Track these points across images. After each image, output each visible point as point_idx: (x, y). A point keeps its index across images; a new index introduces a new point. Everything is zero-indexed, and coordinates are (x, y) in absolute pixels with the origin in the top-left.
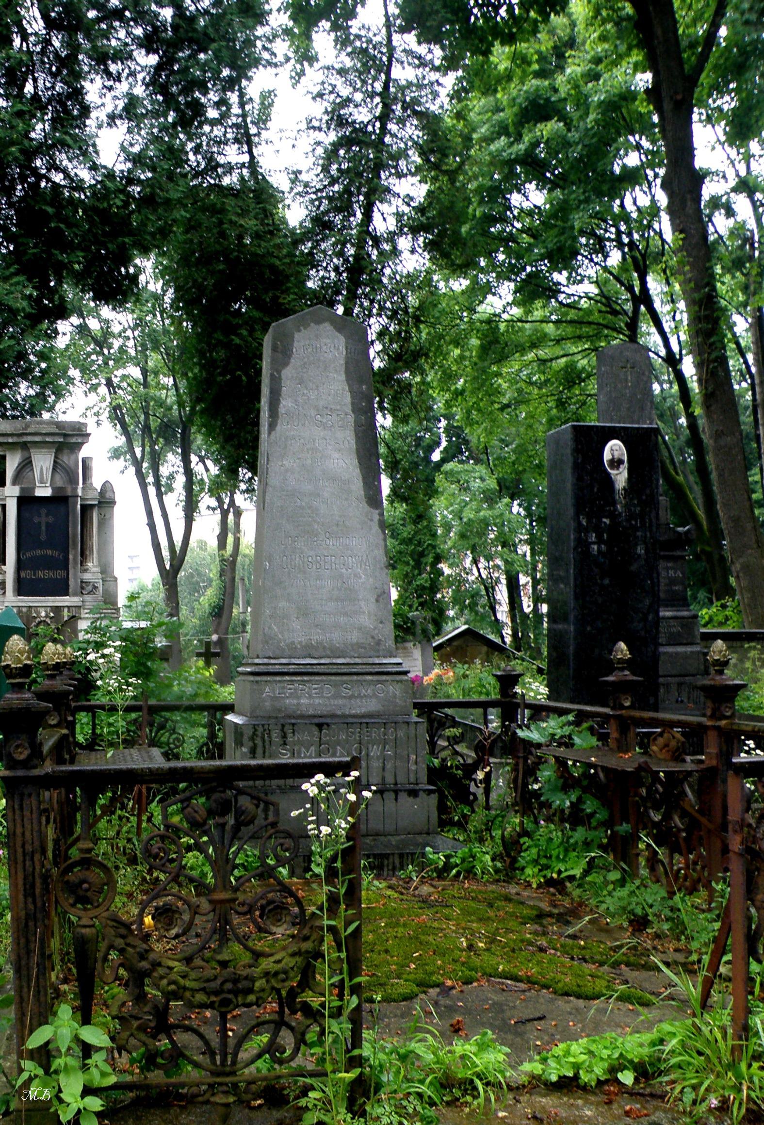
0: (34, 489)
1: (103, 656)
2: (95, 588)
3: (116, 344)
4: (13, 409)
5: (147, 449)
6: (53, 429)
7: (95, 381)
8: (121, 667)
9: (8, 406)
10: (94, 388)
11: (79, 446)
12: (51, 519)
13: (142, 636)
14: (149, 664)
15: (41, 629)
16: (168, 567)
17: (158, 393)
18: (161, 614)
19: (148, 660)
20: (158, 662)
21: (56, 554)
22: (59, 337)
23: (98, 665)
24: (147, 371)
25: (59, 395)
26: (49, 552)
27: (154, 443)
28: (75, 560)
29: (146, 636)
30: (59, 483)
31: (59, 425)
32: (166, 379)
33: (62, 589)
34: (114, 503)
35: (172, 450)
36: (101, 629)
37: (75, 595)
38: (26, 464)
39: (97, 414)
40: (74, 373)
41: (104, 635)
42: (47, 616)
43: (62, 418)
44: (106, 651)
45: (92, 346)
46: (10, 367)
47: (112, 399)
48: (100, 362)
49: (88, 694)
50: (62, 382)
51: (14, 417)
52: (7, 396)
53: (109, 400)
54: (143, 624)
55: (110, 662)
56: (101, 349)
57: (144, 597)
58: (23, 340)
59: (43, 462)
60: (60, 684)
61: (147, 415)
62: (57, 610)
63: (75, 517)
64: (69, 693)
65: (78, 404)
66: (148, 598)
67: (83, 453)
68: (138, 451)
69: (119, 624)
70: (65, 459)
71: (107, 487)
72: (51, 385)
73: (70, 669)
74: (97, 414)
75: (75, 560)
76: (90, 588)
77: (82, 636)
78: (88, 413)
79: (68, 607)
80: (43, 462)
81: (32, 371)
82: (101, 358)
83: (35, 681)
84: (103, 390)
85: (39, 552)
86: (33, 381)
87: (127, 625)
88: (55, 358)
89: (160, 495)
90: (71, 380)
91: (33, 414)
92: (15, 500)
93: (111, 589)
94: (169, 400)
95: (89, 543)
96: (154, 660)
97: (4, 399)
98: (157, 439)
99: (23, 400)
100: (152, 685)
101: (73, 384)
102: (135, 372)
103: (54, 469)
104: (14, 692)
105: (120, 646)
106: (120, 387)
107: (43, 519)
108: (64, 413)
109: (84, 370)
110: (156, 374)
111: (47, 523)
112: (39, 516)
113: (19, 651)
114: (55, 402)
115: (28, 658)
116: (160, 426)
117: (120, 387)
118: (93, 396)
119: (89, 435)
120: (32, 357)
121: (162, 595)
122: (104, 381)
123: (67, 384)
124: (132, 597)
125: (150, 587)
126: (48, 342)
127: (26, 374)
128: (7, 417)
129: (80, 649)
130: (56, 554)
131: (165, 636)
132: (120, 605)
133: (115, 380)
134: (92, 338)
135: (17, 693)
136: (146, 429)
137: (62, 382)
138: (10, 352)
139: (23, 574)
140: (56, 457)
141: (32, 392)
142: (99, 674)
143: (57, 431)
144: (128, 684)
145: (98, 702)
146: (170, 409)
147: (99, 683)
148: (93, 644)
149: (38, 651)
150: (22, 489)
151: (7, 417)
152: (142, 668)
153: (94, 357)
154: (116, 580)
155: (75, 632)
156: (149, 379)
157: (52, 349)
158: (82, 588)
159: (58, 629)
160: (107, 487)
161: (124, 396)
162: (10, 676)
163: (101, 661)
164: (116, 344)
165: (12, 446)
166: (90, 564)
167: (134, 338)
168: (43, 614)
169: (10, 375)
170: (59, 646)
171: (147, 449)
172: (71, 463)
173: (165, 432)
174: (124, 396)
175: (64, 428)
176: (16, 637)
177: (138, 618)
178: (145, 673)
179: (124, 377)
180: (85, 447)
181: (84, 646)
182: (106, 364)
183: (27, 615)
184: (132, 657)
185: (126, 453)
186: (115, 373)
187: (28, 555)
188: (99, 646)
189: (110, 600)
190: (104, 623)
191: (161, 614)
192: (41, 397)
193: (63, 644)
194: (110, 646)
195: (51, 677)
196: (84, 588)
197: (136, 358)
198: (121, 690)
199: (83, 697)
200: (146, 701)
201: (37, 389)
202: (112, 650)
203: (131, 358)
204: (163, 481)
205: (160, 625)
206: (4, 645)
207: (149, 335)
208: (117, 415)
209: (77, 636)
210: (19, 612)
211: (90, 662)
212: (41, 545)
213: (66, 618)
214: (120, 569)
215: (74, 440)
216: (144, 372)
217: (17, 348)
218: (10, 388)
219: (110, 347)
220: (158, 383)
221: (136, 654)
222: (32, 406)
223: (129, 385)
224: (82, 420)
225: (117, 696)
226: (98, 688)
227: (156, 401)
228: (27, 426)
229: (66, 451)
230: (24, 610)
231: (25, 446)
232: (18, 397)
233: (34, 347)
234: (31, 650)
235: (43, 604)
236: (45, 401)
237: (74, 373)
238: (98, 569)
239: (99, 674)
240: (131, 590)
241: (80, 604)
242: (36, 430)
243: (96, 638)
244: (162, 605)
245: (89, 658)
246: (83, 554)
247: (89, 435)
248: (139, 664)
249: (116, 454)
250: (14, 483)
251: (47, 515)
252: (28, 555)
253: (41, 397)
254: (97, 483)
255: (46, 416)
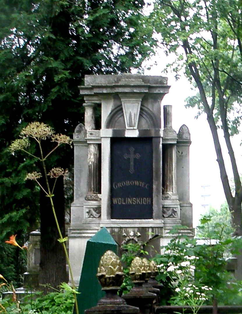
0: (124, 131)
1: (181, 268)
2: (174, 212)
3: (192, 12)
4: (107, 66)
5: (217, 98)
6: (140, 82)
7: (174, 43)
8: (195, 277)
9: (103, 63)
10: (173, 48)
11: (161, 96)
12: (138, 156)
13: (213, 251)
14: (218, 274)
15: (130, 246)
16: (234, 195)
17: (225, 53)
18: (228, 233)
19: (217, 271)
20: (226, 273)
21: (142, 184)
22: (145, 7)
23: (176, 275)
24: (216, 35)
25: (144, 54)
26: (137, 183)
27: (222, 93)
28: (158, 189)
29: (216, 251)
30: (145, 126)
31: (144, 79)
32: (232, 42)
33: (146, 212)
34: (189, 142)
35: (237, 99)
36: (179, 246)
37: (158, 218)
38: (118, 111)
39: (176, 70)
40: (157, 36)
41: (182, 251)
42: (135, 235)
43: (147, 73)
44: (183, 264)
45: (172, 14)
46: (105, 31)
47: (188, 57)
48: (178, 27)
49: (169, 299)
50: (147, 44)
51: (108, 72)
52: (102, 55)
53: (185, 58)
54: (214, 242)
55: (187, 273)
56: (179, 16)
57: (215, 220)
58: (115, 9)
59: (131, 109)
60: (145, 291)
61: (216, 70)
62: (143, 230)
63: (158, 154)
64: (153, 298)
65: (160, 62)
66: (218, 220)
67: (165, 101)
68: (209, 100)
69: (193, 242)
70: (150, 107)
71: (183, 130)
72: (138, 46)
73: (154, 279)
74: (176, 70)
75: (158, 189)
76: (170, 212)
77: (163, 252)
78: (169, 69)
79: (152, 228)
80: (131, 109)
81: (122, 34)
82: (179, 24)
83: (125, 289)
84: (181, 50)
85: (128, 183)
86: (123, 43)
87: (200, 242)
88: (142, 24)
89: (227, 136)
90: (154, 42)
91: (123, 70)
92: (109, 140)
93: (187, 213)
94: (234, 59)
95: (169, 175)
96: (222, 272)
97: (100, 57)
98: (225, 90)
99: (116, 58)
100: (221, 292)
101: (156, 45)
102: (207, 36)
103: (141, 115)
104: (107, 297)
105: (195, 260)
106: (194, 48)
107: (131, 155)
108: (149, 69)
109: (165, 34)
110: (224, 37)
111: (135, 159)
112: (129, 153)
113: (112, 264)
114: (142, 60)
115: (119, 270)
116: (227, 80)
117: (194, 48)
118: (172, 54)
119: (169, 87)
120: (122, 24)
121: (229, 218)
122: (181, 43)
123: (151, 46)
124: (205, 220)
125: (219, 212)
126: (136, 11)
127: (117, 37)
128: (102, 73)
129: (162, 262)
130: (142, 184)
131: (232, 252)
132: (194, 226)
133: (191, 42)
134: (172, 7)
135: (110, 298)
136: (216, 82)
137: (147, 44)
138: (105, 19)
139: (115, 201)
140: (142, 105)
141: (122, 52)
142: (177, 283)
143: (143, 84)
144: (201, 291)
145: (177, 306)
146: (236, 65)
147: (178, 290)
148: (173, 258)
149: (127, 264)
150: (114, 132)
151: (102, 73)
152: (213, 278)
153: (173, 23)
154: (191, 205)
155: (158, 248)
156: (219, 41)
157: (139, 16)
158: (164, 212)
159: (144, 246)
160: (183, 130)
161: (198, 55)
162: (104, 284)
163: (179, 272)
164: (192, 12)
165: (107, 96)
166: (170, 193)
167: (206, 8)
168: (132, 234)
169: (104, 38)
170: (145, 260)
171: (217, 98)
172: (155, 110)
173: (231, 85)
174: (198, 55)
175: (149, 82)
176: (109, 252)
177: (209, 237)
178: (214, 282)
179: (198, 40)
180: (166, 97)
181: (165, 259)
182: (183, 29)
183: (119, 234)
184: (204, 269)
185: (199, 102)
186: (191, 36)
187: (119, 185)
188: (177, 259)
189: (186, 222)
190: (182, 241)
191: (228, 233)
192: (130, 55)
193: (148, 258)
194: (186, 260)
195: (139, 285)
196: (165, 212)
197: (208, 24)
198: (195, 296)
199: (164, 301)
200: (216, 305)
201: (127, 49)
202: (188, 263)
203: (204, 25)
204: (230, 125)
205: (227, 242)
206: (100, 259)
207: (218, 6)
208: (192, 70)
209: (159, 252)
210: (112, 232)
211: (170, 273)
212: (130, 177)
213: (150, 237)
214: (194, 198)
215: (156, 91)
216: (215, 36)
217: (111, 16)
218: (105, 48)
219: (186, 16)
220: (226, 45)
221: (207, 267)
222: (123, 63)
223: (202, 46)
224: (164, 75)
225: (192, 301)
226: (177, 294)
227: (224, 59)
228: (119, 80)
229: (150, 100)
230: (116, 230)
231: (117, 96)
232: (111, 56)
233: (124, 15)
234: (122, 263)
235: (131, 225)
236: (134, 59)
237: (157, 36)
238: (176, 197)
239: (177, 283)
240: (204, 214)
241: (162, 225)
242: (126, 83)
243: (175, 253)
244: (229, 226)
245: (169, 269)
246: (164, 184)
247: (169, 87)
248: (210, 274)
249: (192, 102)
250: (108, 126)
251: (135, 153)
252: (119, 185)
253: (130, 55)
254: (175, 126)
255: (134, 71)
